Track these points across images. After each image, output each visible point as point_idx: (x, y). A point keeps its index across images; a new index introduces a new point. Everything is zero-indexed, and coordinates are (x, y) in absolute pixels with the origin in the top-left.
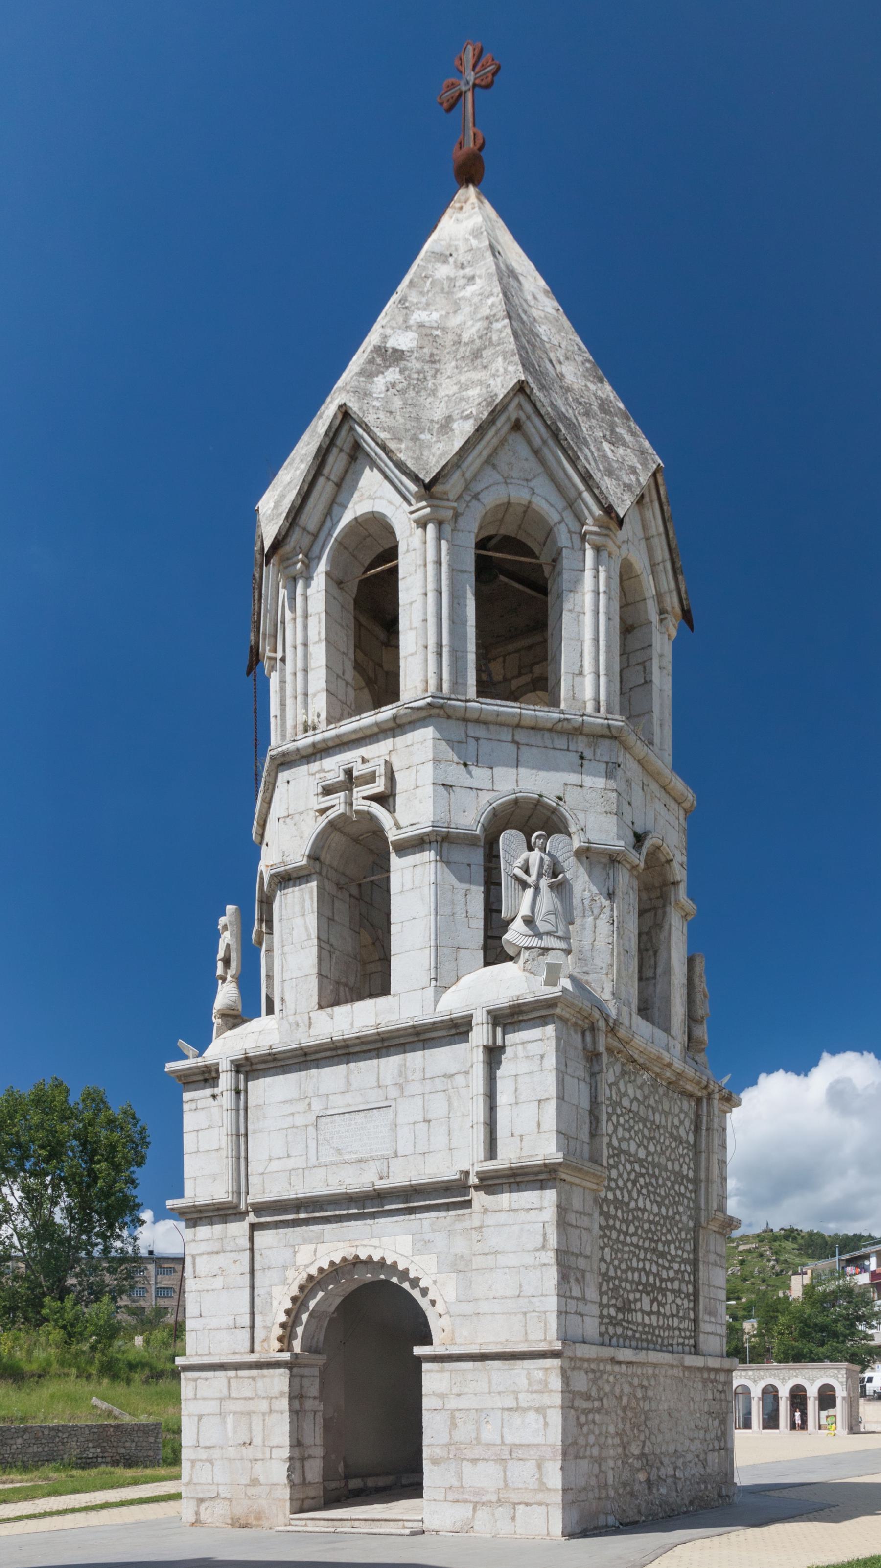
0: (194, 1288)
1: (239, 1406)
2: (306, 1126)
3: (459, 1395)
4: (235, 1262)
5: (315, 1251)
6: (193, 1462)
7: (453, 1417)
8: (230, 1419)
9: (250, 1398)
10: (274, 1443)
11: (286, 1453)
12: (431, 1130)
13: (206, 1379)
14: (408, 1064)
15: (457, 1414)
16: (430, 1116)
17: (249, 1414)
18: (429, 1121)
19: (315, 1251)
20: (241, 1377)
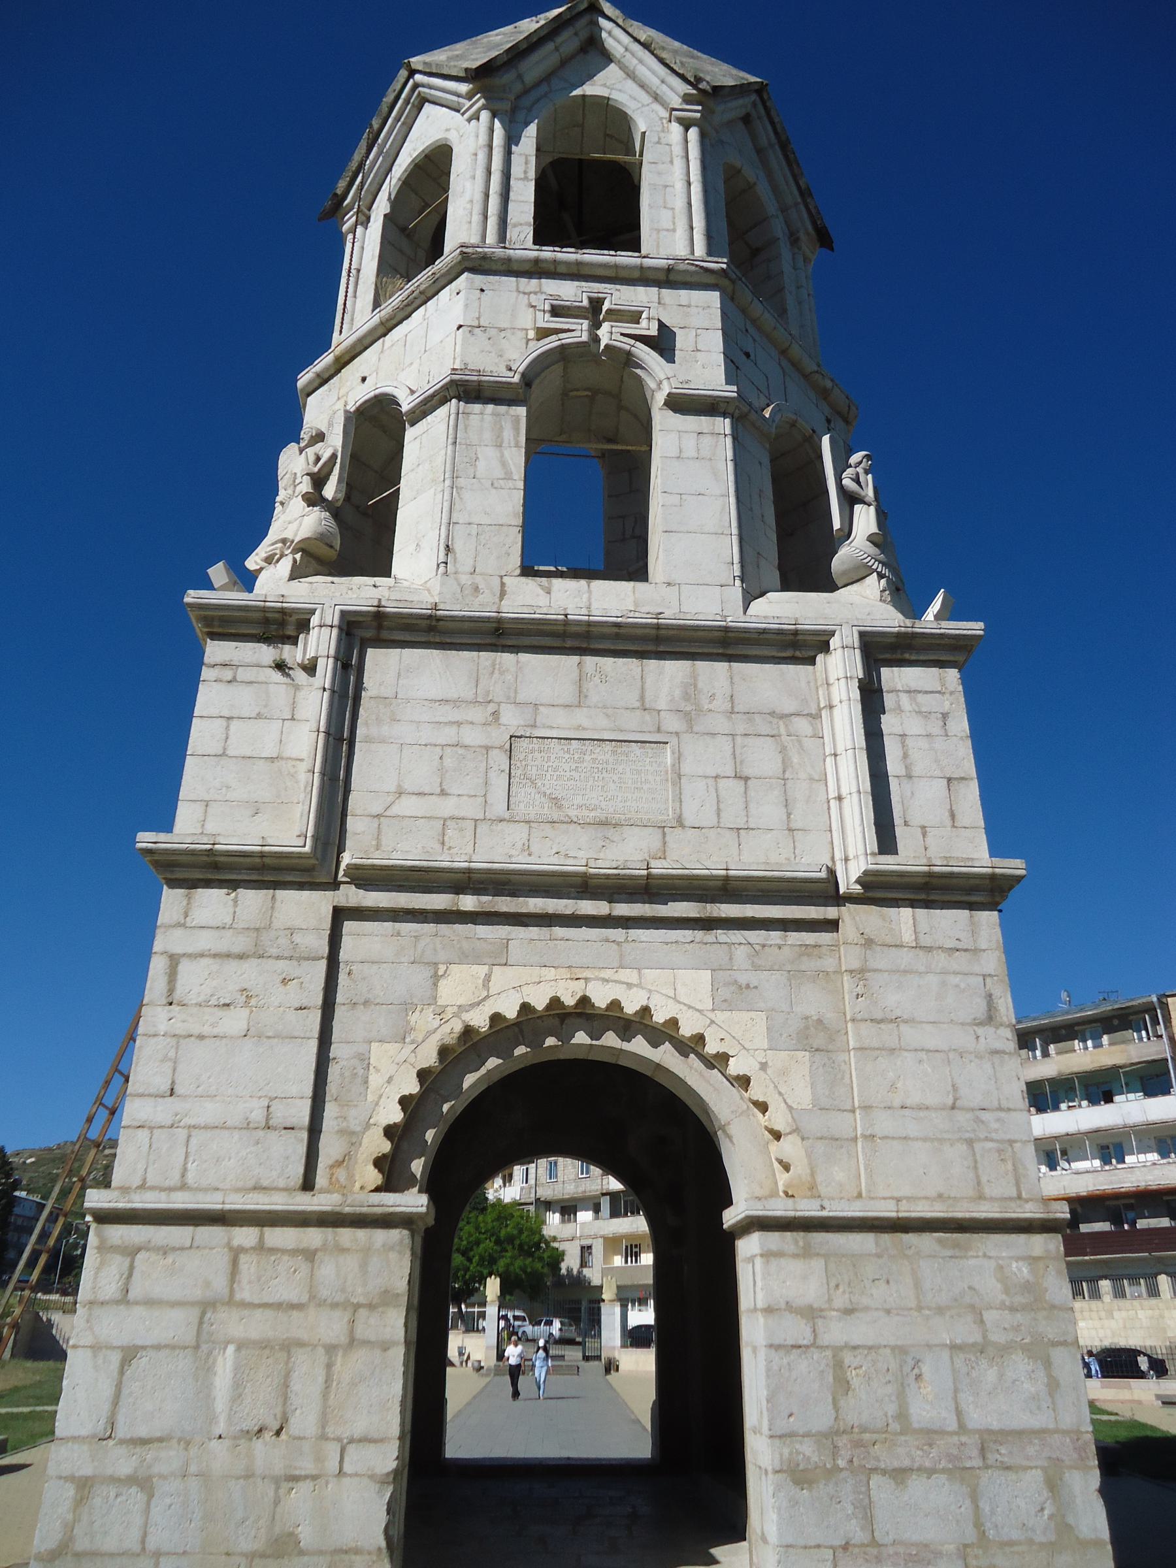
0: (162, 1028)
1: (258, 1326)
2: (487, 748)
3: (849, 1312)
4: (284, 982)
5: (488, 978)
6: (84, 1486)
7: (838, 1365)
8: (225, 1363)
9: (293, 1307)
10: (359, 1426)
11: (387, 1457)
12: (751, 793)
13: (165, 1251)
14: (700, 685)
15: (848, 1358)
16: (747, 771)
17: (289, 1346)
18: (747, 779)
19: (488, 978)
20: (273, 1250)
